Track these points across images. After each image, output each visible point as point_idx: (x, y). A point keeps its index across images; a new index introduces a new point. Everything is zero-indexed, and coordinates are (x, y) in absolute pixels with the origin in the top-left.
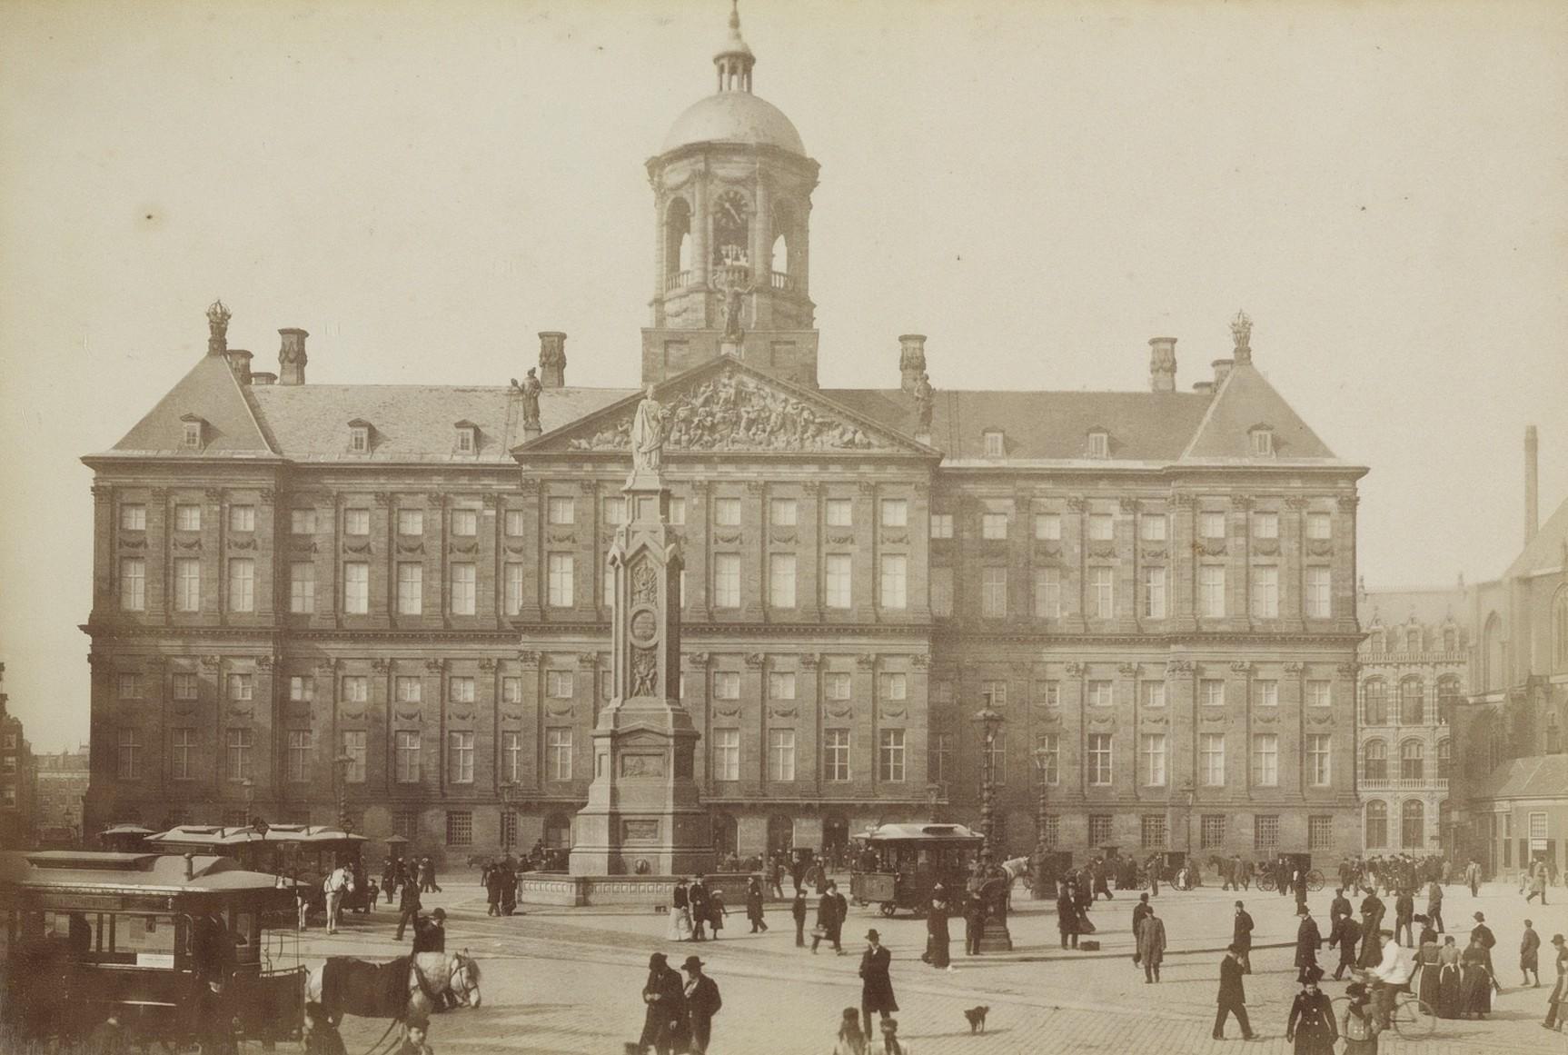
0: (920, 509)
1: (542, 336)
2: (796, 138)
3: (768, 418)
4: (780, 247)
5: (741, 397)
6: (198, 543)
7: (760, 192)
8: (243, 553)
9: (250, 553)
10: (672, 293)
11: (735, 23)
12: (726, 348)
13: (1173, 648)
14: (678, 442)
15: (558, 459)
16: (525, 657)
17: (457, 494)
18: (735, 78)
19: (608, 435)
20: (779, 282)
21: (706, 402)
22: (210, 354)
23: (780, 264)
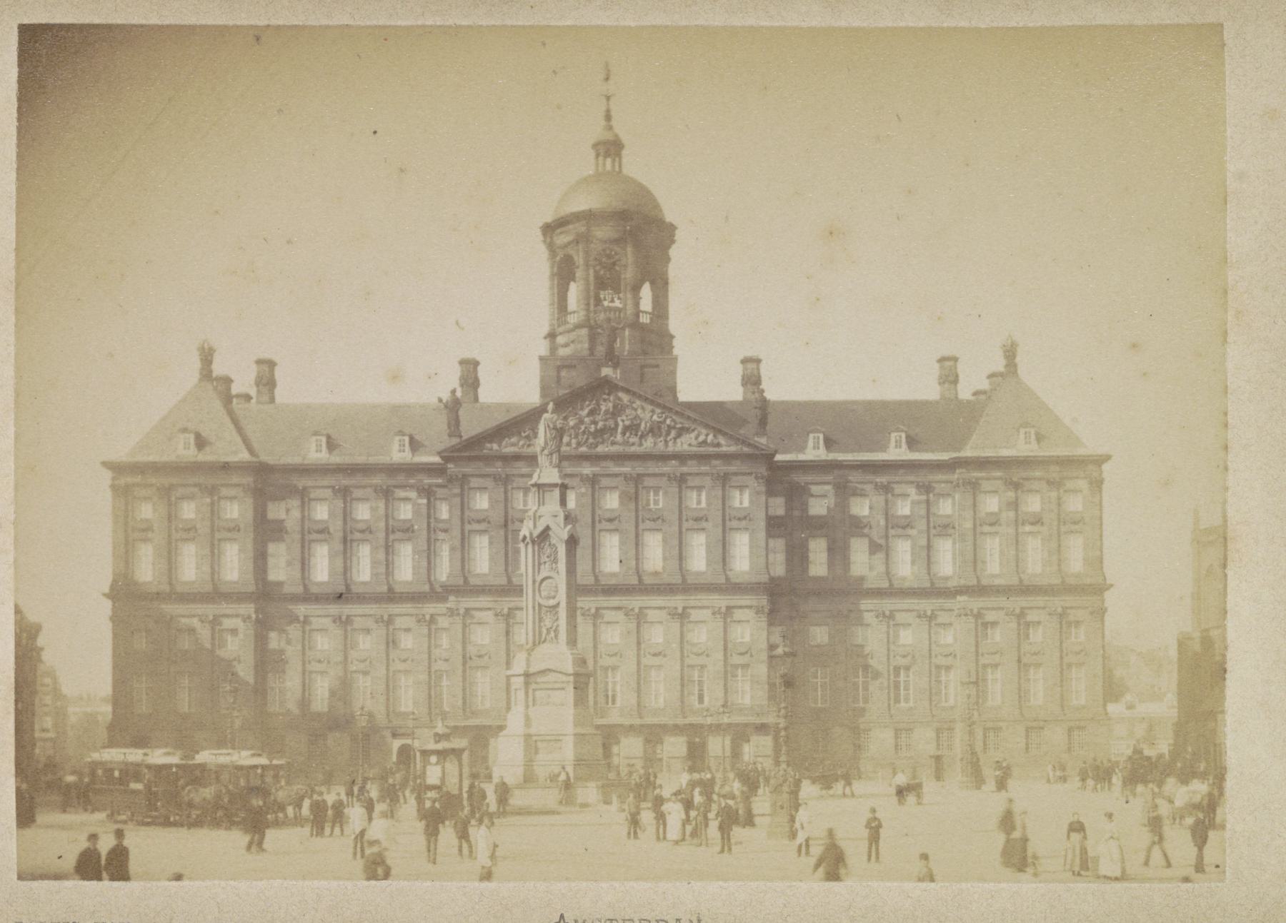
0: (758, 493)
1: (462, 362)
2: (657, 206)
3: (639, 425)
4: (646, 292)
6: (194, 528)
7: (629, 249)
8: (229, 535)
10: (561, 329)
11: (608, 117)
12: (606, 371)
13: (959, 598)
14: (569, 444)
16: (452, 612)
17: (395, 487)
18: (609, 161)
19: (514, 440)
20: (645, 319)
21: (592, 413)
22: (200, 380)
23: (646, 302)
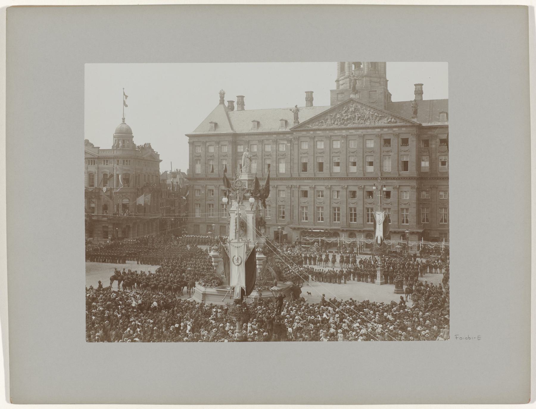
5: (356, 110)
9: (226, 158)
14: (337, 124)
15: (303, 131)
19: (317, 123)
